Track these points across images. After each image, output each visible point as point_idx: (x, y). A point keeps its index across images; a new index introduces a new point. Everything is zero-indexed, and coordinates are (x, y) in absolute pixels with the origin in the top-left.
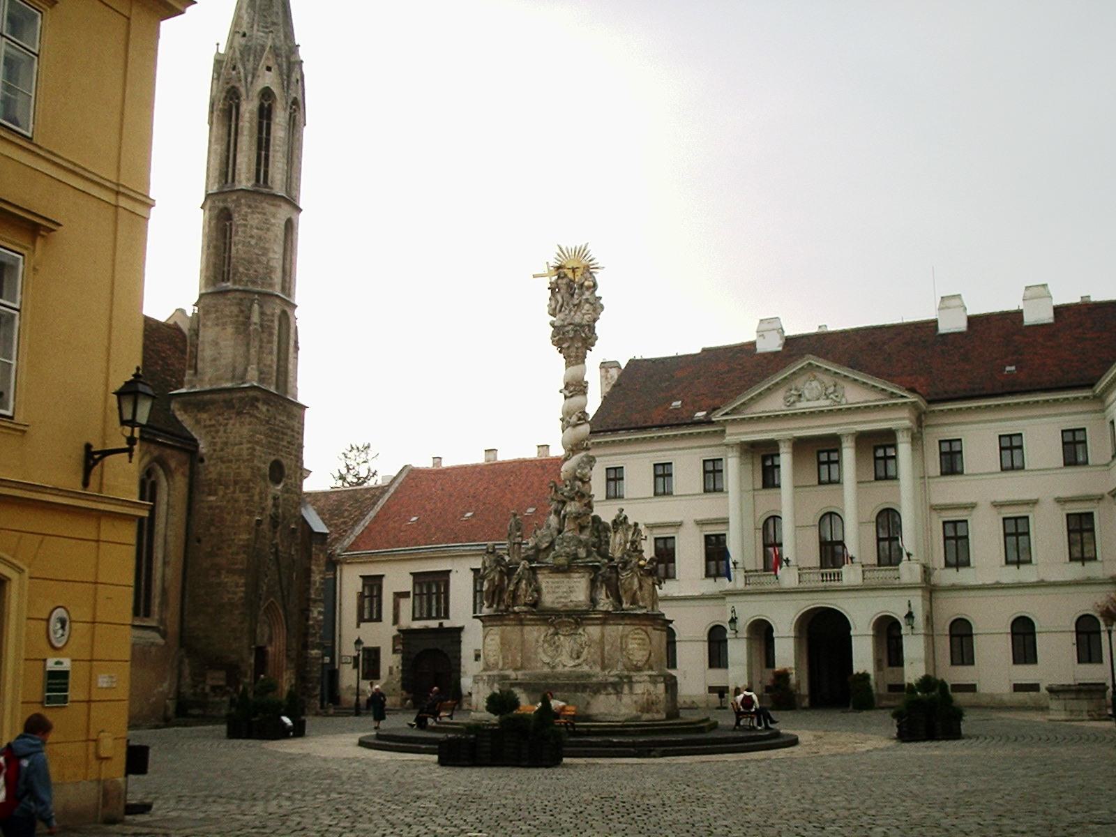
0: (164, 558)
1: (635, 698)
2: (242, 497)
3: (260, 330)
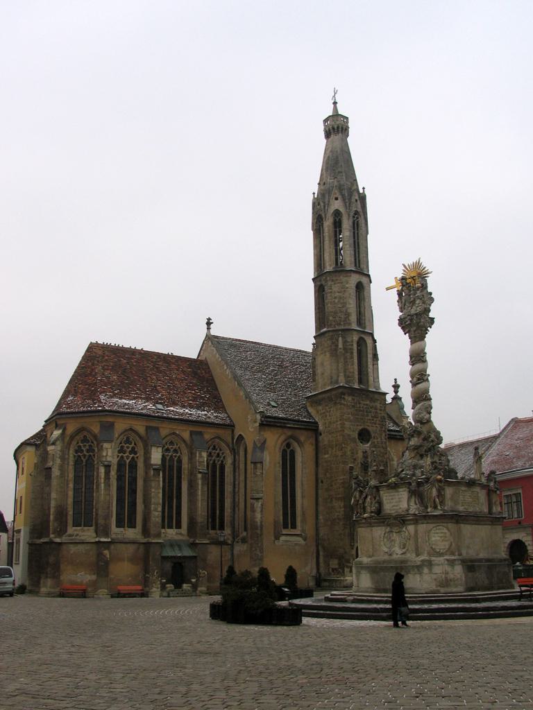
0: (302, 493)
1: (434, 576)
2: (339, 453)
3: (343, 352)
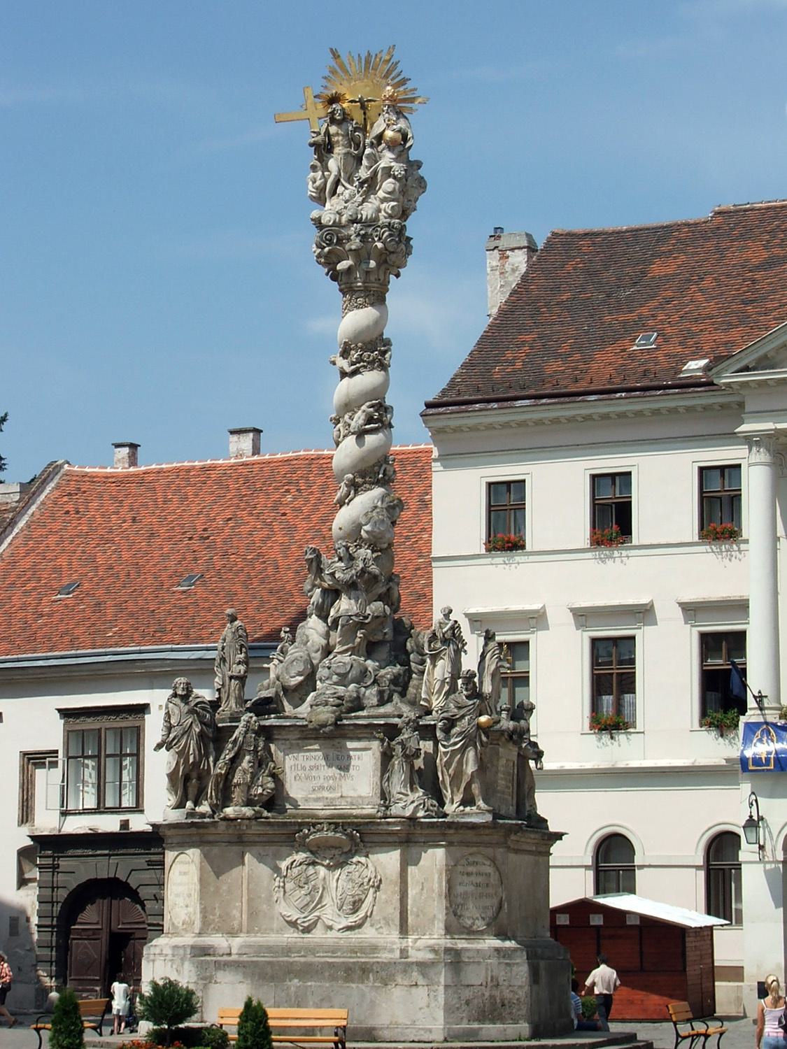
1: (467, 994)
